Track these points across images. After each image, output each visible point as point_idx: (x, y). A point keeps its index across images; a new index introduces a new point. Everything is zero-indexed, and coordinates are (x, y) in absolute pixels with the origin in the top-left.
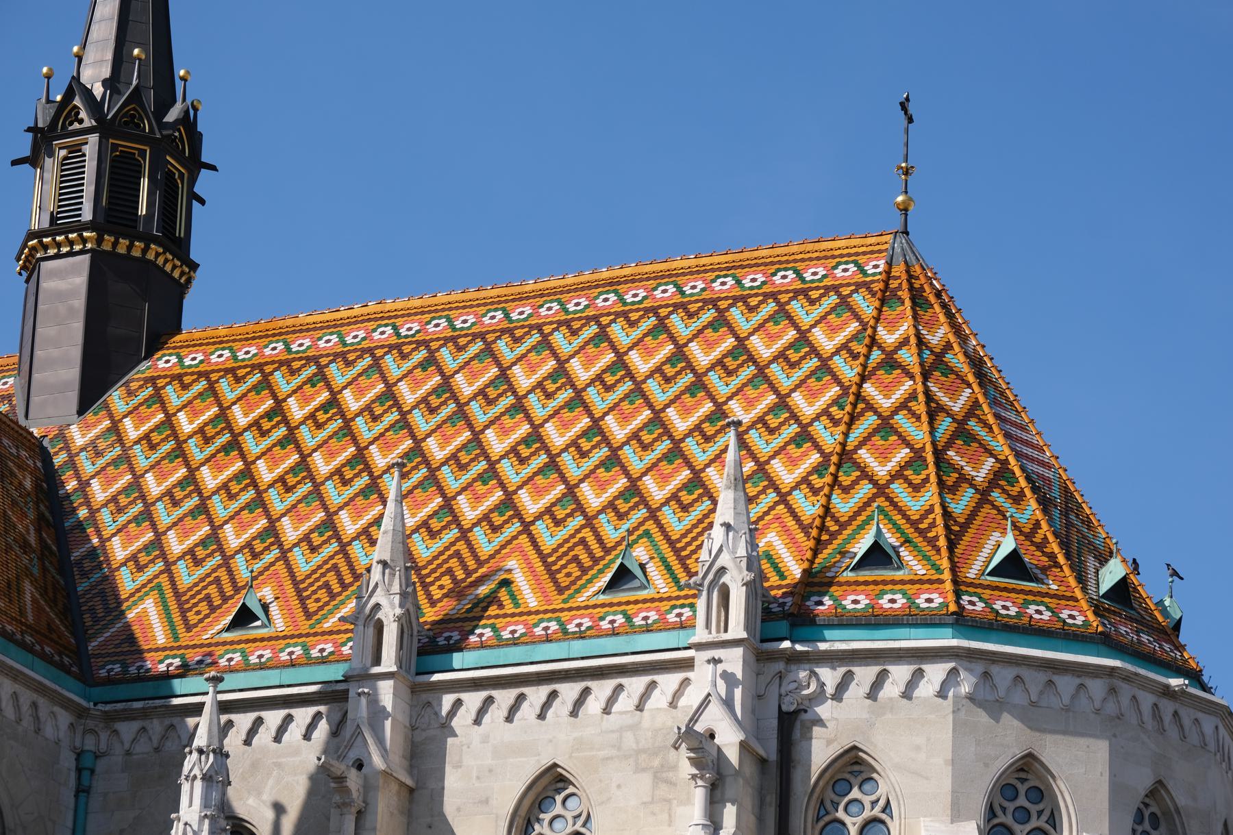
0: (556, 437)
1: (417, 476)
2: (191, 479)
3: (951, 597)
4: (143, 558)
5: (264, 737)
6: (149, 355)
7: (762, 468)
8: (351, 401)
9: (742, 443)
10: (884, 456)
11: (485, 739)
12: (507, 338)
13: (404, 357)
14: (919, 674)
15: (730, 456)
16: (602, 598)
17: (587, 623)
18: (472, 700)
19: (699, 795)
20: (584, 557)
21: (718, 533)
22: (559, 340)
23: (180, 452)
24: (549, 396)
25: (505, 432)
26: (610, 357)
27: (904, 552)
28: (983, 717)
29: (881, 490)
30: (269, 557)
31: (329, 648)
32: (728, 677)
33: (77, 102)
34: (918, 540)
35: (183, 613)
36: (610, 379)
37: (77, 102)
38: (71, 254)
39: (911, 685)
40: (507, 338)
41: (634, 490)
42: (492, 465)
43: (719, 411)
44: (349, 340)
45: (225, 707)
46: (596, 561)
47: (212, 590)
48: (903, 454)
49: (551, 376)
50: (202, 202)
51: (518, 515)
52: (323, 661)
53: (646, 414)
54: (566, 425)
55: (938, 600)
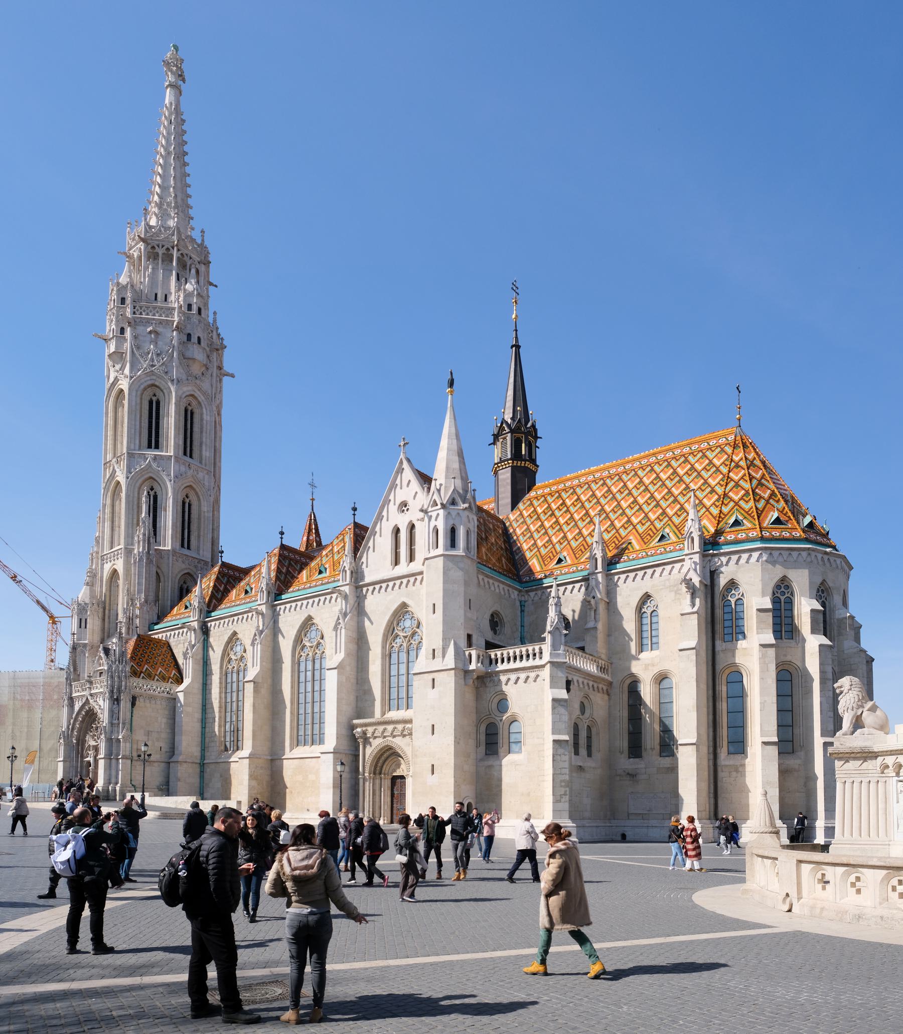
0: (641, 500)
1: (603, 517)
2: (542, 525)
3: (759, 533)
4: (532, 548)
5: (568, 592)
7: (701, 501)
8: (583, 498)
9: (695, 496)
10: (737, 493)
11: (627, 587)
14: (751, 556)
15: (692, 499)
16: (657, 544)
17: (653, 552)
18: (623, 577)
19: (688, 596)
20: (651, 533)
21: (689, 522)
22: (640, 473)
23: (539, 518)
24: (638, 489)
25: (627, 501)
26: (655, 475)
27: (744, 521)
28: (770, 566)
29: (737, 504)
30: (565, 544)
31: (583, 567)
32: (695, 563)
34: (748, 517)
35: (544, 561)
37: (504, 425)
39: (748, 559)
40: (625, 474)
41: (664, 513)
43: (687, 487)
45: (558, 585)
46: (655, 534)
47: (551, 555)
48: (743, 492)
52: (582, 570)
54: (643, 497)
55: (755, 534)
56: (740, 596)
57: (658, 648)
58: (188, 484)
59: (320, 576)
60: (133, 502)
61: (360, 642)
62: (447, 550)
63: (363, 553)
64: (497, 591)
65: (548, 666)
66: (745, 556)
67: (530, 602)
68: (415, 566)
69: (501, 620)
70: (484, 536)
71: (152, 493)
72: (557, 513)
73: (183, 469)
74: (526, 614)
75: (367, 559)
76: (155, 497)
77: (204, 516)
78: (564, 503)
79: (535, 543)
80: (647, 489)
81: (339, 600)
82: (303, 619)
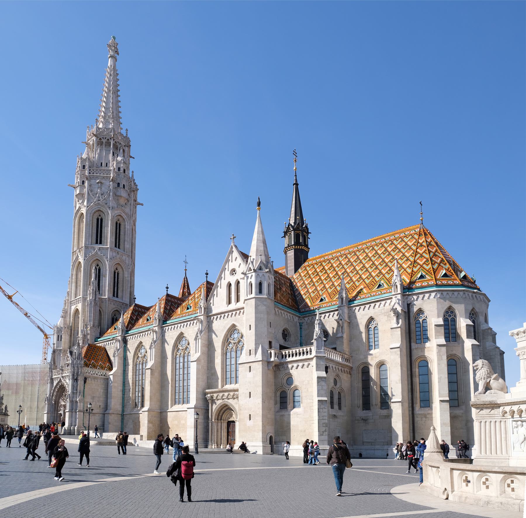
0: (367, 266)
1: (346, 275)
2: (312, 281)
3: (435, 282)
4: (306, 293)
5: (326, 317)
6: (304, 263)
7: (401, 265)
8: (335, 265)
9: (397, 262)
10: (421, 261)
11: (360, 314)
12: (358, 252)
13: (342, 257)
14: (430, 295)
15: (396, 264)
16: (377, 290)
17: (374, 294)
18: (358, 308)
19: (395, 318)
20: (373, 284)
21: (395, 277)
22: (366, 250)
23: (310, 277)
24: (365, 259)
26: (375, 252)
27: (426, 276)
28: (442, 301)
30: (324, 291)
31: (335, 303)
32: (398, 299)
33: (290, 227)
34: (428, 273)
35: (313, 301)
36: (375, 255)
37: (290, 227)
38: (291, 250)
39: (429, 297)
40: (358, 252)
41: (380, 272)
42: (357, 272)
43: (393, 258)
44: (333, 256)
45: (320, 314)
46: (375, 284)
47: (317, 297)
48: (425, 260)
49: (366, 256)
50: (309, 239)
51: (362, 279)
52: (334, 305)
53: (381, 260)
54: (368, 264)
55: (433, 283)
56: (425, 318)
57: (378, 348)
58: (117, 263)
59: (188, 311)
60: (87, 272)
61: (209, 346)
62: (257, 295)
63: (211, 298)
64: (286, 317)
65: (315, 359)
66: (427, 295)
67: (305, 323)
68: (240, 305)
69: (289, 333)
70: (278, 287)
71: (98, 268)
72: (320, 274)
73: (114, 254)
74: (303, 330)
75: (213, 301)
76: (99, 270)
77: (126, 279)
78: (324, 268)
79: (308, 291)
80: (370, 259)
81: (198, 324)
82: (178, 334)
